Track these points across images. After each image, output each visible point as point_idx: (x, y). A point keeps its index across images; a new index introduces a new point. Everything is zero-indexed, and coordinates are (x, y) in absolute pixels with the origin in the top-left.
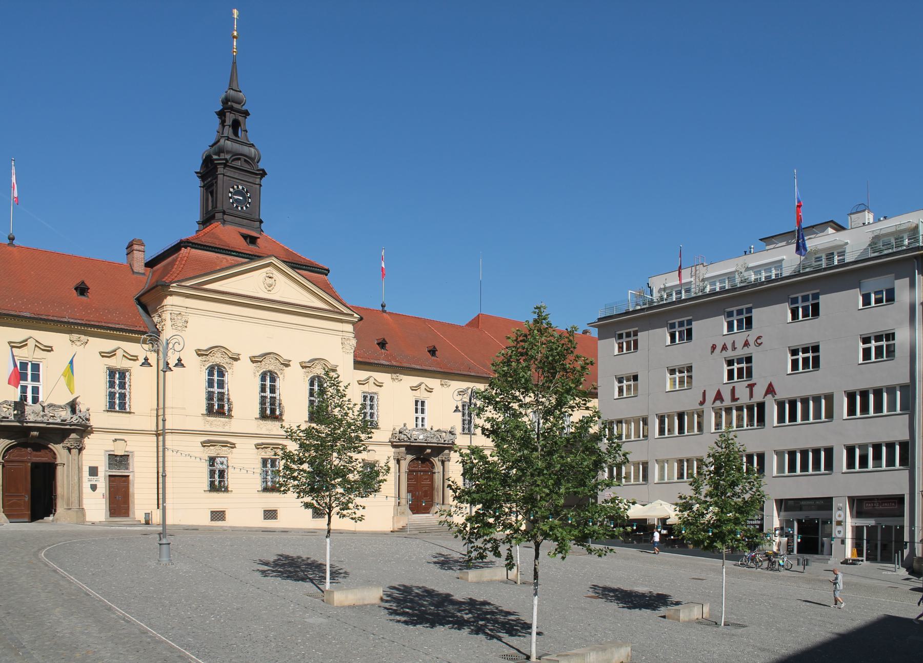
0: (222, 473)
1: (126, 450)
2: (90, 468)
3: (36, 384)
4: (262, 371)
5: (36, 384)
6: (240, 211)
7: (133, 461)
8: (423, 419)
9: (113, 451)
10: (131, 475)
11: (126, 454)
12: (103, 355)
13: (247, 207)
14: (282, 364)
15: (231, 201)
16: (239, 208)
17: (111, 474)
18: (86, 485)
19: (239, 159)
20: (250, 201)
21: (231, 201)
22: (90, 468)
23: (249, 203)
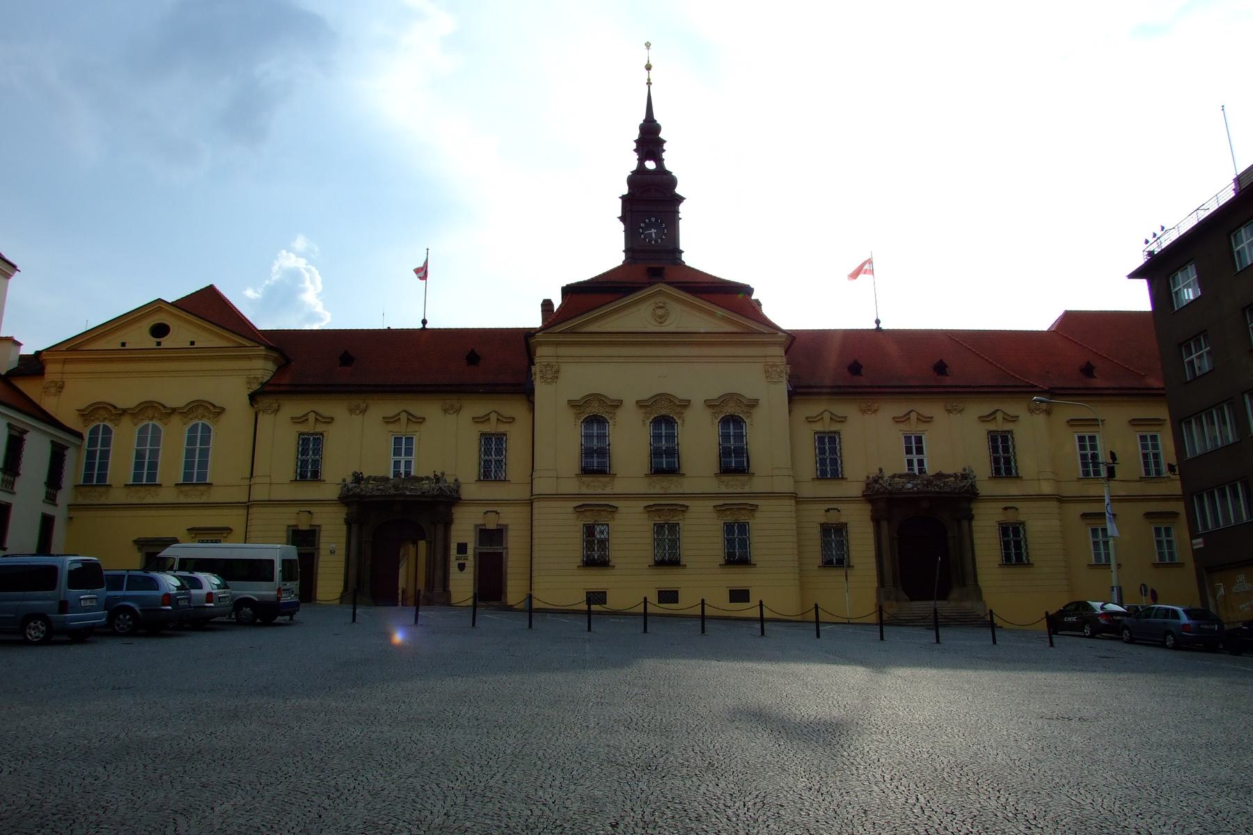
0: (603, 543)
1: (499, 523)
2: (458, 544)
3: (409, 458)
4: (653, 417)
9: (484, 525)
10: (505, 551)
11: (499, 527)
12: (477, 420)
14: (679, 406)
15: (643, 236)
17: (482, 551)
18: (454, 565)
21: (643, 236)
22: (458, 544)
23: (665, 235)
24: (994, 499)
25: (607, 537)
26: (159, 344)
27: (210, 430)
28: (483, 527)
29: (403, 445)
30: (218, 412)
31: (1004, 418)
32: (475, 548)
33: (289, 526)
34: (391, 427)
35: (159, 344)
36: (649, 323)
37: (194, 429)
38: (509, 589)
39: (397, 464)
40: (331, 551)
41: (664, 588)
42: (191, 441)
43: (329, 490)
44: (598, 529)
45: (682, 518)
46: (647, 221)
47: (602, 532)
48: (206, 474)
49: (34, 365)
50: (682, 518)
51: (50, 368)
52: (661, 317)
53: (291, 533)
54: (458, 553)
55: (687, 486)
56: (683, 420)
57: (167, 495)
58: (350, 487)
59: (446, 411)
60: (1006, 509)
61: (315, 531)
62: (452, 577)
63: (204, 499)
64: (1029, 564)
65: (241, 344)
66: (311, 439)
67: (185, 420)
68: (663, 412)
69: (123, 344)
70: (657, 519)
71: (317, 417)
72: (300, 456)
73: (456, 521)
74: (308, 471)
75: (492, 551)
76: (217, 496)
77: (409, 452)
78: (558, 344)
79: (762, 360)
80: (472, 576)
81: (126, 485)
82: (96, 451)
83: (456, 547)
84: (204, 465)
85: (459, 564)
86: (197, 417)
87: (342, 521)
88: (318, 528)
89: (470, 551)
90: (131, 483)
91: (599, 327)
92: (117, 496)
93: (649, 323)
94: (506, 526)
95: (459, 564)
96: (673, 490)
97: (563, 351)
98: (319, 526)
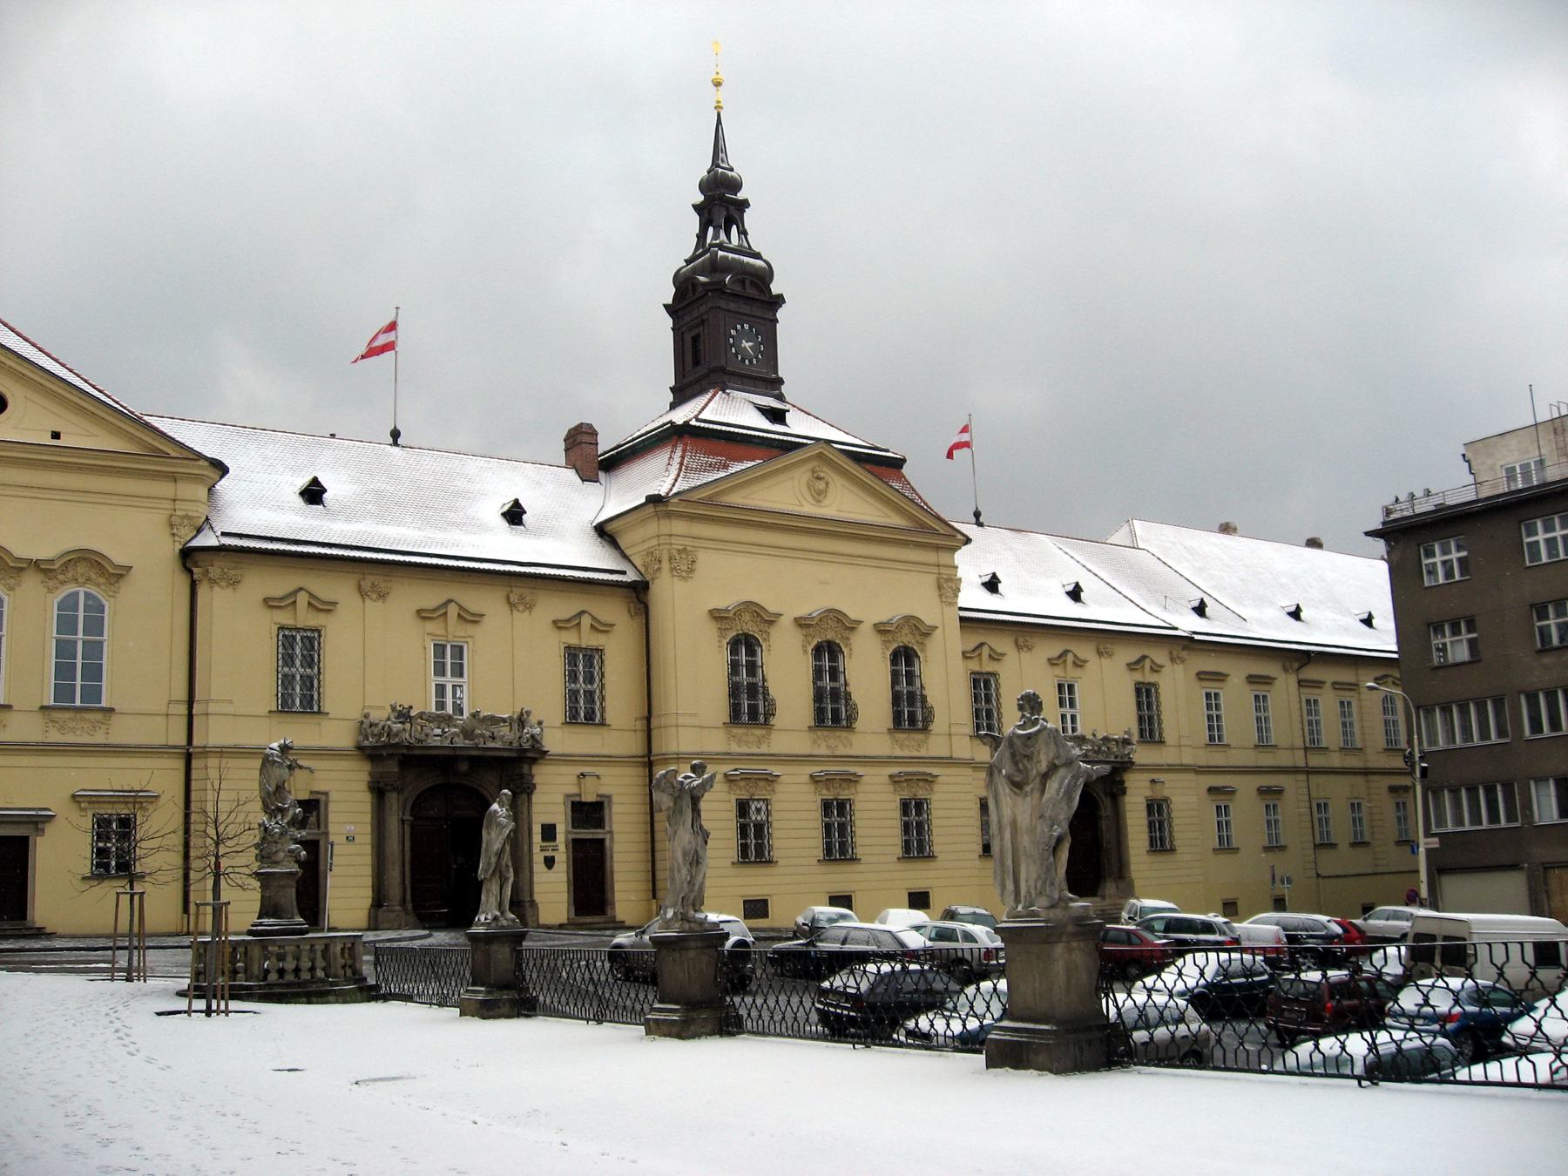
2: (543, 826)
7: (610, 810)
8: (1073, 718)
9: (580, 795)
10: (608, 837)
11: (599, 799)
18: (538, 858)
20: (762, 349)
24: (1146, 768)
25: (764, 818)
27: (101, 609)
28: (577, 799)
29: (449, 659)
30: (115, 575)
31: (990, 655)
32: (567, 832)
34: (431, 627)
36: (805, 499)
37: (69, 604)
38: (618, 896)
39: (441, 689)
40: (347, 838)
41: (751, 896)
42: (66, 623)
43: (336, 732)
44: (753, 808)
45: (854, 791)
46: (739, 327)
47: (758, 810)
48: (99, 689)
50: (854, 791)
52: (820, 493)
54: (544, 839)
55: (936, 745)
56: (851, 650)
58: (395, 730)
59: (363, 594)
61: (317, 801)
62: (536, 878)
63: (99, 738)
65: (163, 452)
66: (298, 638)
67: (51, 584)
68: (829, 637)
70: (824, 792)
71: (462, 613)
72: (280, 669)
73: (539, 789)
75: (590, 837)
76: (122, 732)
79: (935, 570)
80: (564, 877)
81: (43, 708)
82: (76, 642)
84: (94, 672)
85: (546, 858)
87: (363, 786)
88: (323, 798)
89: (561, 837)
90: (52, 703)
91: (744, 498)
93: (805, 499)
94: (609, 797)
95: (546, 858)
96: (841, 751)
98: (326, 794)
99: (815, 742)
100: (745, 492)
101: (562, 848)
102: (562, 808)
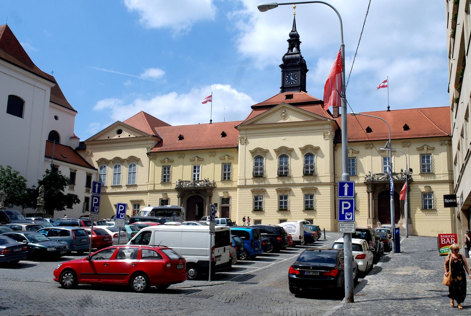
0: (261, 203)
5: (198, 173)
6: (292, 85)
11: (228, 197)
13: (295, 82)
14: (289, 151)
15: (287, 81)
16: (292, 83)
19: (290, 62)
26: (119, 136)
28: (223, 198)
29: (196, 169)
32: (220, 205)
33: (160, 199)
35: (119, 136)
39: (194, 176)
46: (289, 75)
49: (83, 146)
51: (88, 147)
52: (284, 116)
53: (160, 201)
57: (124, 189)
60: (426, 186)
63: (135, 190)
64: (435, 210)
68: (283, 153)
69: (109, 137)
70: (280, 193)
73: (214, 196)
74: (166, 179)
76: (138, 189)
77: (198, 171)
78: (246, 130)
83: (218, 206)
86: (131, 162)
89: (218, 206)
91: (261, 122)
92: (109, 190)
97: (248, 132)
99: (278, 181)
100: (261, 121)
101: (219, 208)
102: (219, 200)
